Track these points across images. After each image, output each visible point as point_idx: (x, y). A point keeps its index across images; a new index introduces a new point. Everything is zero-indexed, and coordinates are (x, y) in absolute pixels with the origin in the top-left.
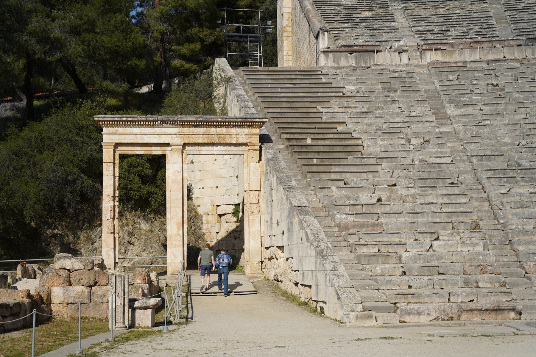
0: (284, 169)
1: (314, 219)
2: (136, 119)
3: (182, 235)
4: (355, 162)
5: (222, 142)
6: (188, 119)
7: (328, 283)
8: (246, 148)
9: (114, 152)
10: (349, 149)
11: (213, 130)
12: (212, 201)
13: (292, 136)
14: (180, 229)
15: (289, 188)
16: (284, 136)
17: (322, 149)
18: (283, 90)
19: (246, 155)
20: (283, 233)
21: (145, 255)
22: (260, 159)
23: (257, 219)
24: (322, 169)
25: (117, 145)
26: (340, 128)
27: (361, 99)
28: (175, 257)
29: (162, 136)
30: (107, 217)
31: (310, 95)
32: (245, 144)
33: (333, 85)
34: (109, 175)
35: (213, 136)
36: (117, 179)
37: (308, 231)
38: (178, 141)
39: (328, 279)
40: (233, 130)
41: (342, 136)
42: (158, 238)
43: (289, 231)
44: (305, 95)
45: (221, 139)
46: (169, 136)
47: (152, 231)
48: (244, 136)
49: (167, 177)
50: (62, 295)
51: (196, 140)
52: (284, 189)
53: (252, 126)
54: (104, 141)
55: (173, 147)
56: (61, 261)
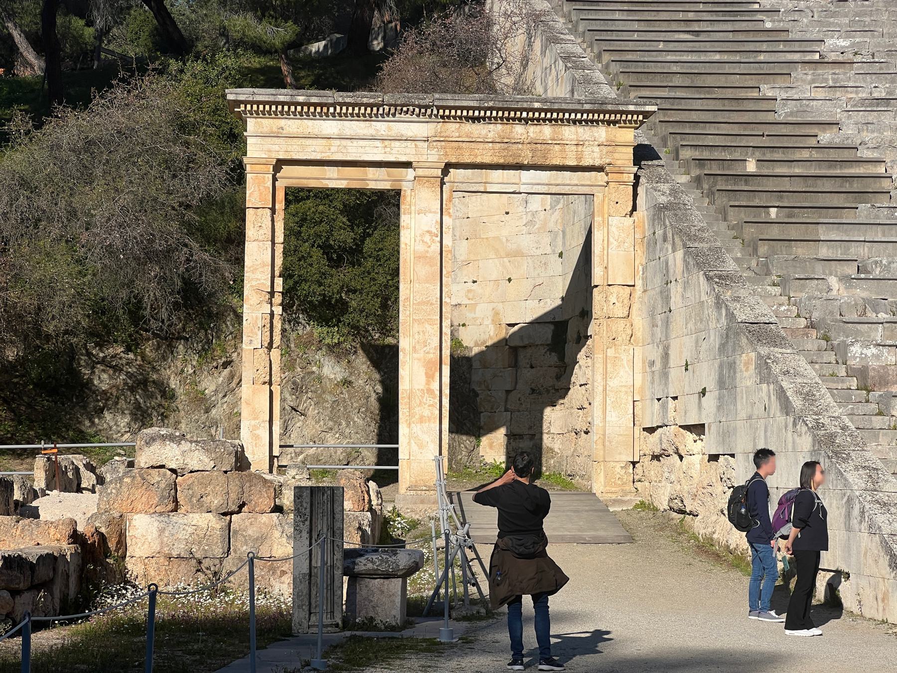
0: (702, 230)
1: (797, 357)
2: (330, 101)
3: (438, 393)
4: (877, 217)
5: (540, 162)
6: (458, 104)
7: (855, 522)
8: (601, 177)
9: (275, 179)
10: (856, 186)
11: (519, 130)
12: (497, 314)
13: (706, 154)
14: (433, 377)
15: (720, 277)
16: (686, 154)
17: (786, 185)
18: (671, 46)
19: (601, 195)
20: (703, 392)
21: (331, 440)
22: (634, 208)
23: (625, 358)
24: (794, 232)
25: (280, 164)
26: (826, 137)
27: (866, 68)
28: (421, 446)
29: (394, 144)
30: (255, 342)
31: (737, 58)
32: (600, 169)
33: (791, 36)
34: (261, 238)
35: (520, 146)
36: (279, 249)
37: (785, 384)
38: (434, 157)
39: (856, 511)
40: (569, 133)
41: (833, 155)
42: (363, 401)
43: (721, 384)
44: (726, 57)
45: (539, 153)
46: (409, 143)
47: (350, 383)
48: (597, 149)
49: (402, 246)
50: (155, 534)
51: (476, 156)
52: (709, 279)
53: (615, 123)
54: (249, 154)
55: (420, 172)
56: (156, 447)
